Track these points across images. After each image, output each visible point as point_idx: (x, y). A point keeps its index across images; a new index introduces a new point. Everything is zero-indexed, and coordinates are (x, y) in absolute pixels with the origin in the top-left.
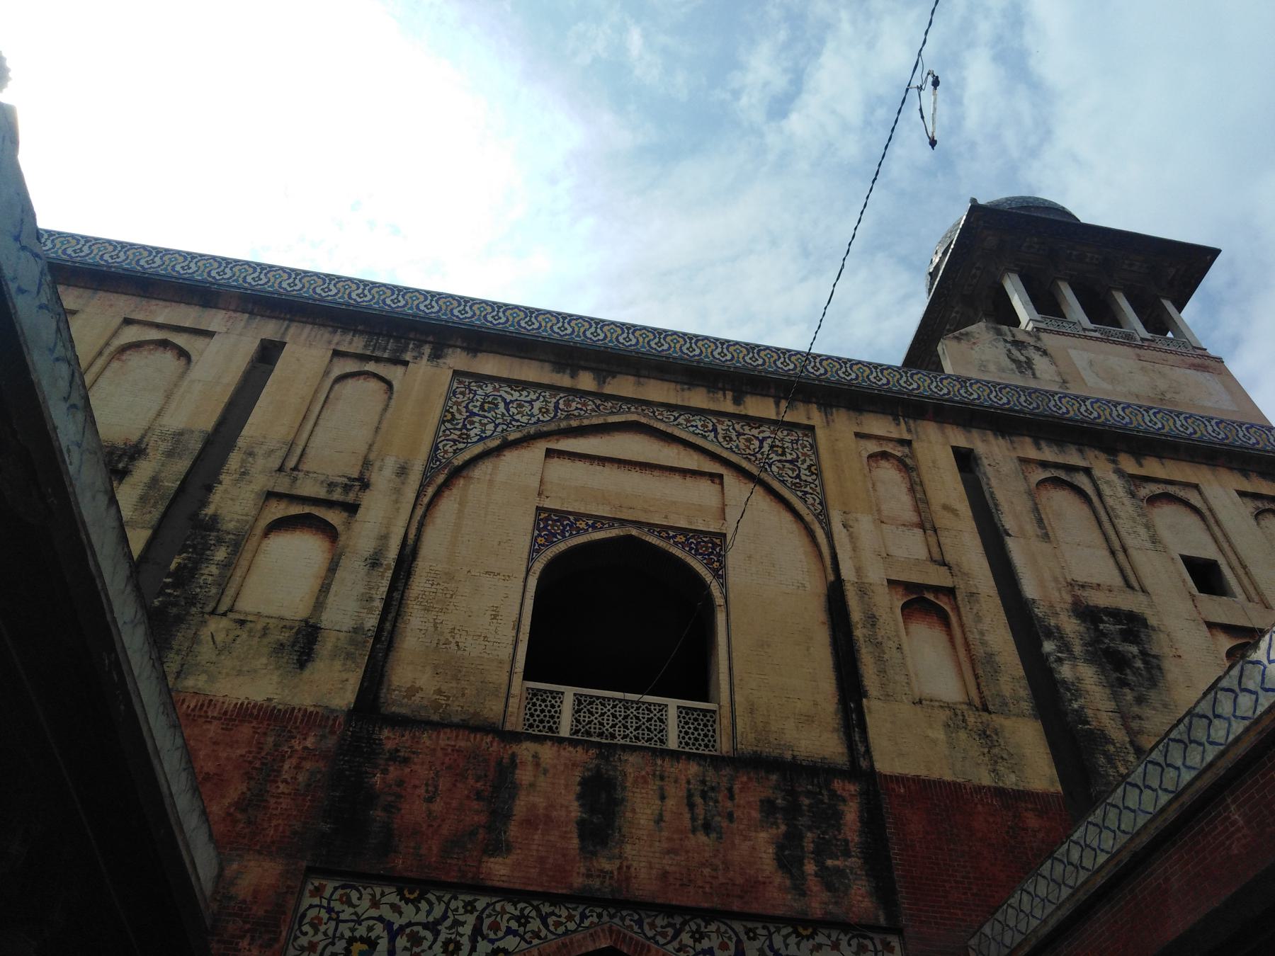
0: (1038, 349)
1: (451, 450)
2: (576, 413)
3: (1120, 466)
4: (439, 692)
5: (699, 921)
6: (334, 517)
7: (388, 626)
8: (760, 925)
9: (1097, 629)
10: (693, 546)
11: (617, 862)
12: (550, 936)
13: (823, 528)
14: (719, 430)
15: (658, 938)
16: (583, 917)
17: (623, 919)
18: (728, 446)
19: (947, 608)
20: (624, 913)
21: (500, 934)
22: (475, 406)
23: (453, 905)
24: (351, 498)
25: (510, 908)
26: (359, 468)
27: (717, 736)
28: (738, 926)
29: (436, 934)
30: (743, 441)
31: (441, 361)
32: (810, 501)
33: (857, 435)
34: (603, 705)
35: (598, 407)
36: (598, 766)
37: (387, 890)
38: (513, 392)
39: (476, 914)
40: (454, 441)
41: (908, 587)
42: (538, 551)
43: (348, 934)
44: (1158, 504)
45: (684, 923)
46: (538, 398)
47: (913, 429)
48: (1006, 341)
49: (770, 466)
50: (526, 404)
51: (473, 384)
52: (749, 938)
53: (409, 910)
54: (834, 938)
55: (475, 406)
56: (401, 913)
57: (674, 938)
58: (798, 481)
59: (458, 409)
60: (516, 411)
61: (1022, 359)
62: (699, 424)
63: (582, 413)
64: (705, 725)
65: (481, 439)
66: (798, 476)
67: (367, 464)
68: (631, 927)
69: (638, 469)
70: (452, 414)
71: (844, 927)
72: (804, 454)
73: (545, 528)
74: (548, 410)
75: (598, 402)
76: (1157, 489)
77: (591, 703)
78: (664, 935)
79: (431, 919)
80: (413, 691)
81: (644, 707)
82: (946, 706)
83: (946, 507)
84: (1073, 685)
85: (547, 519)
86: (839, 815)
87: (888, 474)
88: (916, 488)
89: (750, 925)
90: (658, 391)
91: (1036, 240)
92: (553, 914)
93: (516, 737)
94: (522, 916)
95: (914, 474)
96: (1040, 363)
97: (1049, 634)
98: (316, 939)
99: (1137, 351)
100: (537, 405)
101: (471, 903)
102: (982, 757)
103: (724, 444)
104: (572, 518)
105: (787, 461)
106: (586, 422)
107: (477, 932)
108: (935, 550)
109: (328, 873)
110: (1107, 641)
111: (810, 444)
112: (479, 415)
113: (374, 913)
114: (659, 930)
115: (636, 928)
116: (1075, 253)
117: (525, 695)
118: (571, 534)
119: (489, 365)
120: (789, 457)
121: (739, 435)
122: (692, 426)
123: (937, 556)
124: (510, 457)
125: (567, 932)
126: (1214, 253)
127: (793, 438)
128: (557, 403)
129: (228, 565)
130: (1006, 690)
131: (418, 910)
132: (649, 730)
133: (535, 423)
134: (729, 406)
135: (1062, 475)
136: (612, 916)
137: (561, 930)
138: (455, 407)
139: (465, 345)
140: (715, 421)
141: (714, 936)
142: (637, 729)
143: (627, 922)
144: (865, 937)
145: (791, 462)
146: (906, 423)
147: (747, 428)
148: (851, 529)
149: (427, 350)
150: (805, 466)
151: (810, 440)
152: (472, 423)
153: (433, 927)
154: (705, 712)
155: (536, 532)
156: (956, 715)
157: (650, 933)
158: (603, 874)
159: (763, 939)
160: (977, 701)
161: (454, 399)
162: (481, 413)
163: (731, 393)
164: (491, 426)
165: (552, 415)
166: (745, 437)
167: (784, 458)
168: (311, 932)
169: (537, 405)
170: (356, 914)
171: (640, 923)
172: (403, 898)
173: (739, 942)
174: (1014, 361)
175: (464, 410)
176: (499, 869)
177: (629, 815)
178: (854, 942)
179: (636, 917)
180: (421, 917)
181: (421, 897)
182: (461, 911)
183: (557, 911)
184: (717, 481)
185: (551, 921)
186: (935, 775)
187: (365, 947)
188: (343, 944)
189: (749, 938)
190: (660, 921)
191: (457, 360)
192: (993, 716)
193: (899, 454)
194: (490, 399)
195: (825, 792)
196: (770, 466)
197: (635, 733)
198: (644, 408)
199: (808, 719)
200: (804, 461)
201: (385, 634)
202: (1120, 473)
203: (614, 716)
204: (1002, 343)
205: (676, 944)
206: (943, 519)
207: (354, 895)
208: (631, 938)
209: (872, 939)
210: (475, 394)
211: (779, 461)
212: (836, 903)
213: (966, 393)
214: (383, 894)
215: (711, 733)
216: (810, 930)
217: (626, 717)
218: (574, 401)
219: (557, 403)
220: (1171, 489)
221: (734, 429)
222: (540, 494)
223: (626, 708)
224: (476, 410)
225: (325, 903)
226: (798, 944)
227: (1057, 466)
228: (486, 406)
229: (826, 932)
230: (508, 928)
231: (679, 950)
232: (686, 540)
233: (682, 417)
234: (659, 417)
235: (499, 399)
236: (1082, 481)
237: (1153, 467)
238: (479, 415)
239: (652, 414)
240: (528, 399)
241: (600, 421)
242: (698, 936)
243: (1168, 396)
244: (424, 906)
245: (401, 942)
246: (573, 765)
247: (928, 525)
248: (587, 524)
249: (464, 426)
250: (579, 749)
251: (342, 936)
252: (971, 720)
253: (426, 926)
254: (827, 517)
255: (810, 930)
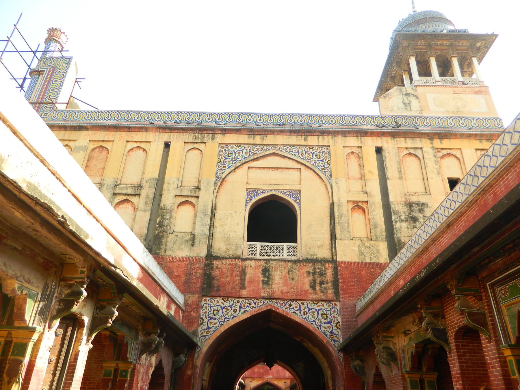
0: (414, 96)
1: (221, 173)
2: (256, 152)
3: (434, 145)
4: (226, 248)
5: (291, 301)
6: (193, 200)
7: (211, 232)
8: (305, 302)
9: (411, 210)
10: (291, 195)
11: (271, 289)
12: (257, 307)
13: (330, 184)
14: (300, 152)
15: (281, 306)
16: (264, 302)
17: (273, 302)
18: (302, 158)
19: (365, 208)
20: (273, 301)
21: (246, 307)
22: (226, 155)
23: (235, 301)
24: (197, 195)
25: (247, 301)
26: (197, 183)
27: (297, 253)
28: (300, 302)
29: (232, 308)
30: (307, 155)
31: (215, 140)
32: (327, 175)
33: (343, 146)
34: (267, 247)
35: (262, 149)
36: (266, 266)
37: (220, 299)
38: (236, 148)
39: (240, 303)
40: (222, 169)
41: (354, 202)
42: (247, 203)
43: (213, 309)
44: (445, 158)
45: (287, 302)
46: (244, 149)
47: (363, 142)
48: (403, 95)
49: (315, 163)
50: (241, 152)
51: (225, 147)
52: (302, 305)
53: (225, 303)
54: (323, 304)
55: (226, 155)
56: (223, 304)
57: (285, 306)
58: (323, 167)
59: (222, 157)
60: (238, 155)
61: (408, 102)
62: (293, 150)
63: (258, 152)
64: (294, 250)
65: (229, 167)
66: (324, 166)
67: (199, 182)
68: (275, 304)
69: (275, 169)
70: (220, 159)
71: (325, 301)
72: (326, 157)
73: (249, 195)
74: (247, 153)
75: (262, 147)
76: (445, 152)
77: (264, 247)
78: (282, 305)
79: (230, 305)
80: (220, 249)
81: (278, 247)
82: (360, 239)
83: (370, 172)
84: (399, 229)
85: (249, 192)
86: (326, 274)
87: (353, 159)
88: (361, 165)
89: (303, 302)
90: (280, 140)
91: (423, 41)
92: (257, 302)
93: (246, 260)
94: (250, 303)
95: (361, 159)
96: (415, 103)
97: (395, 213)
98: (206, 311)
99: (455, 89)
100: (244, 151)
101: (238, 301)
102: (367, 254)
103: (301, 157)
104: (256, 190)
105: (321, 160)
106: (259, 156)
107: (240, 307)
108: (364, 187)
109: (207, 296)
110: (413, 213)
111: (329, 153)
112: (227, 158)
113: (218, 304)
114: (281, 304)
115: (276, 304)
116: (439, 43)
117: (247, 246)
118: (256, 196)
119: (230, 138)
120: (321, 159)
121: (306, 152)
122: (291, 151)
123: (364, 190)
124: (238, 171)
125: (260, 306)
126: (496, 36)
127: (323, 151)
128: (250, 149)
129: (170, 219)
130: (379, 233)
131: (227, 303)
132: (279, 253)
133: (244, 159)
134: (303, 142)
135: (412, 151)
136: (270, 302)
137: (259, 305)
138: (221, 157)
139: (221, 133)
140: (298, 148)
141: (294, 305)
142: (276, 253)
143: (274, 303)
144: (330, 303)
145: (322, 160)
146: (361, 139)
147: (308, 149)
148: (338, 184)
149: (210, 136)
150: (326, 162)
151: (329, 151)
152: (226, 162)
153: (231, 306)
154: (294, 246)
155: (247, 197)
156: (362, 242)
157: (279, 305)
158: (268, 292)
159: (305, 305)
160: (369, 237)
161: (220, 154)
162: (228, 157)
163: (303, 136)
164: (231, 162)
165: (249, 155)
166: (308, 153)
167: (320, 159)
168: (205, 309)
169: (244, 151)
170: (214, 305)
171: (277, 303)
172: (223, 300)
173: (300, 306)
174: (404, 104)
175: (223, 157)
176: (244, 293)
177: (273, 277)
178: (328, 304)
179: (276, 301)
180: (228, 305)
181: (227, 300)
182: (237, 302)
183: (258, 301)
184: (299, 170)
185: (256, 303)
186: (353, 261)
187: (217, 312)
188: (212, 311)
189: (302, 305)
190: (282, 302)
191: (220, 138)
192: (373, 241)
193: (357, 152)
194: (230, 152)
195: (323, 268)
196: (315, 163)
197: (276, 254)
198: (276, 147)
199: (321, 247)
200: (326, 160)
201: (211, 234)
202: (433, 148)
203: (270, 250)
204: (401, 95)
205: (285, 307)
206: (368, 176)
207: (213, 301)
208: (275, 307)
209: (332, 303)
210: (226, 151)
211: (318, 161)
212: (324, 296)
213: (383, 122)
214: (219, 300)
215: (295, 252)
216: (317, 302)
217: (273, 250)
218: (255, 148)
219: (250, 149)
220: (450, 151)
221: (304, 150)
222: (247, 184)
223: (273, 247)
224: (226, 157)
225: (207, 303)
226: (314, 306)
227: (411, 148)
228: (229, 154)
229: (321, 302)
230: (247, 306)
231: (286, 309)
232: (290, 193)
233: (288, 148)
234: (281, 150)
235: (233, 151)
236: (419, 153)
237: (446, 143)
238: (227, 158)
239: (278, 149)
240: (241, 150)
241: (263, 154)
242: (290, 305)
243: (461, 109)
244: (228, 302)
245: (224, 310)
246: (260, 266)
247: (363, 179)
248: (261, 192)
249: (224, 163)
250: (261, 262)
251: (212, 310)
252: (366, 243)
253: (229, 306)
254: (332, 180)
255: (317, 302)
